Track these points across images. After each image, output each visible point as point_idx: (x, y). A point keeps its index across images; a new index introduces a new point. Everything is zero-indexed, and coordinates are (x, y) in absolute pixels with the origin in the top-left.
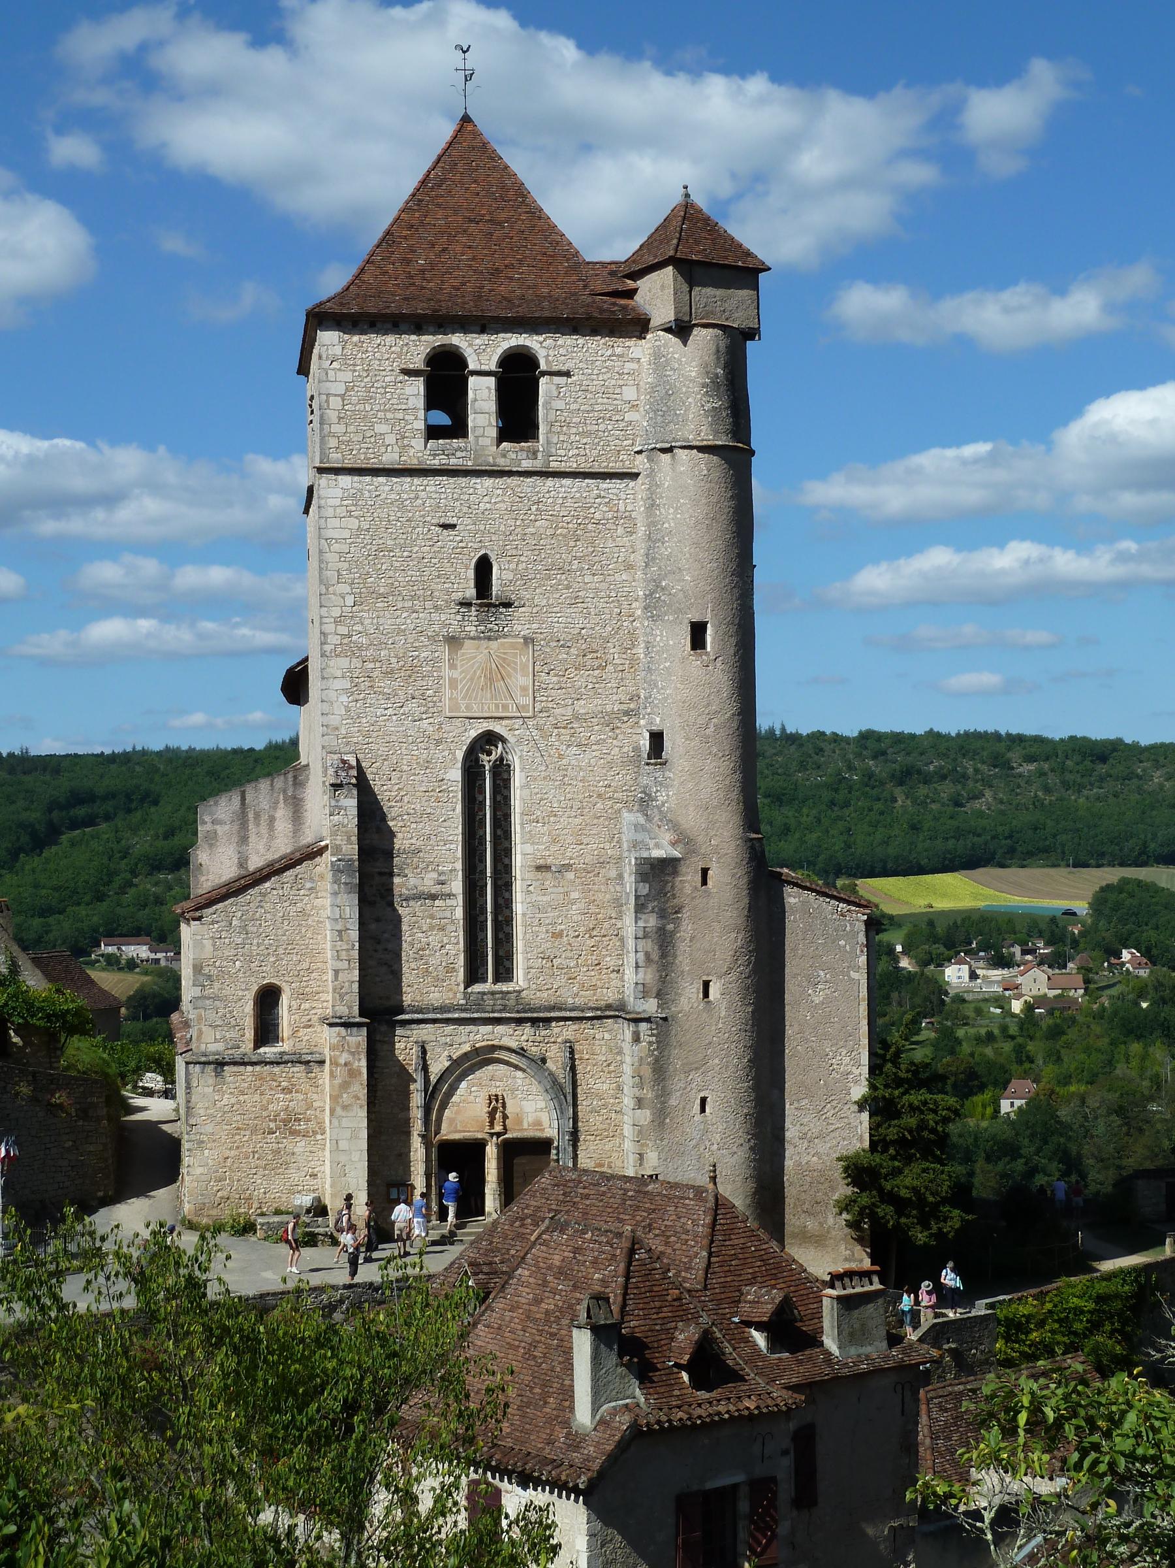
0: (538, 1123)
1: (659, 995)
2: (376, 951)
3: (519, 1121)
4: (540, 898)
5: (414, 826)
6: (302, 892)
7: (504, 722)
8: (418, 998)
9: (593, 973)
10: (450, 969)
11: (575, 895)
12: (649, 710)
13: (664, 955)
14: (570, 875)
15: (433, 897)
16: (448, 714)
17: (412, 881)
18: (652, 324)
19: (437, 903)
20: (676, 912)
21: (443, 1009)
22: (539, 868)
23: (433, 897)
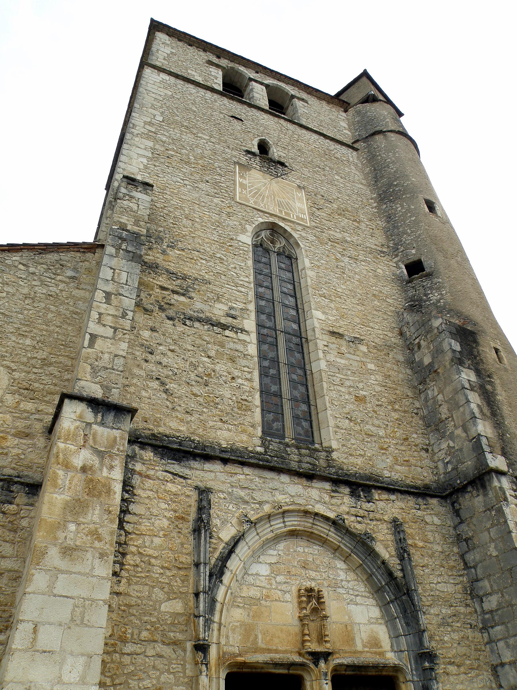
0: (375, 643)
1: (504, 454)
2: (146, 361)
3: (349, 637)
4: (339, 360)
5: (204, 262)
6: (59, 278)
7: (289, 224)
8: (200, 431)
9: (403, 448)
10: (243, 406)
11: (371, 366)
12: (402, 249)
13: (494, 414)
14: (364, 348)
15: (225, 327)
16: (238, 200)
17: (198, 305)
18: (352, 104)
19: (227, 333)
20: (489, 376)
21: (233, 451)
22: (333, 333)
23: (225, 327)
